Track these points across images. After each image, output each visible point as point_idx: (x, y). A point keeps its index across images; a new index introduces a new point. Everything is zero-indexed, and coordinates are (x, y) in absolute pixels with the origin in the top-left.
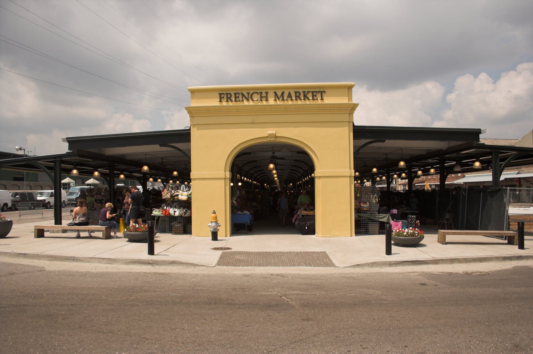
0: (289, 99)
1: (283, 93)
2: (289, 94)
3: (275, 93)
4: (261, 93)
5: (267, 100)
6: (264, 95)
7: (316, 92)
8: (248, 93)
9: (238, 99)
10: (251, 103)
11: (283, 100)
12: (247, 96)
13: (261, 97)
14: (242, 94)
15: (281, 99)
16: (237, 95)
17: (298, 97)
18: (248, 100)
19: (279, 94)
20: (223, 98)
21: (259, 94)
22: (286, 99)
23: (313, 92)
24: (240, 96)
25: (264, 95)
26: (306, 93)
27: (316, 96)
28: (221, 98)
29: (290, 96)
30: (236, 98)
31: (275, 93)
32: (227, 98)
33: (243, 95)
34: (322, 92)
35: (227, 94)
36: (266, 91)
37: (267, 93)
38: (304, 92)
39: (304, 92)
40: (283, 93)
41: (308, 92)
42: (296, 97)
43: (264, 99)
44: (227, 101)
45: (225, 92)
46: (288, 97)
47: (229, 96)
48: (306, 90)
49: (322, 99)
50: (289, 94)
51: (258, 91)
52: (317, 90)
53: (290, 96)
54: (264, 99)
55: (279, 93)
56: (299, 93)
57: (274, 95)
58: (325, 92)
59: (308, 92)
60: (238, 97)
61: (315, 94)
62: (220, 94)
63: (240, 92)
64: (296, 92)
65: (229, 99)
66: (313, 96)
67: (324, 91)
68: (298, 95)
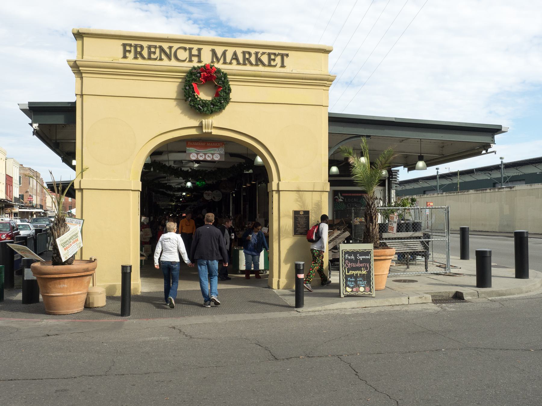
0: (234, 62)
1: (224, 54)
2: (235, 54)
3: (213, 52)
4: (190, 49)
6: (195, 52)
7: (275, 54)
8: (170, 48)
9: (153, 56)
10: (174, 62)
11: (225, 63)
12: (168, 51)
13: (191, 55)
14: (160, 47)
15: (222, 61)
16: (153, 50)
17: (247, 61)
18: (169, 58)
19: (219, 54)
20: (130, 51)
21: (188, 51)
23: (269, 55)
24: (158, 51)
25: (195, 52)
26: (259, 55)
27: (274, 60)
28: (125, 51)
29: (235, 56)
30: (150, 53)
31: (213, 52)
32: (136, 52)
33: (162, 49)
34: (282, 56)
35: (136, 46)
37: (199, 50)
38: (257, 54)
40: (224, 54)
41: (263, 53)
42: (244, 59)
43: (195, 59)
44: (136, 58)
45: (133, 43)
46: (233, 59)
47: (139, 49)
49: (283, 66)
50: (235, 54)
51: (188, 46)
52: (277, 52)
53: (235, 56)
54: (195, 59)
55: (219, 50)
56: (250, 54)
57: (210, 54)
58: (287, 55)
59: (263, 53)
60: (154, 53)
61: (273, 57)
62: (124, 45)
63: (158, 44)
64: (244, 53)
65: (138, 54)
66: (270, 60)
68: (247, 56)
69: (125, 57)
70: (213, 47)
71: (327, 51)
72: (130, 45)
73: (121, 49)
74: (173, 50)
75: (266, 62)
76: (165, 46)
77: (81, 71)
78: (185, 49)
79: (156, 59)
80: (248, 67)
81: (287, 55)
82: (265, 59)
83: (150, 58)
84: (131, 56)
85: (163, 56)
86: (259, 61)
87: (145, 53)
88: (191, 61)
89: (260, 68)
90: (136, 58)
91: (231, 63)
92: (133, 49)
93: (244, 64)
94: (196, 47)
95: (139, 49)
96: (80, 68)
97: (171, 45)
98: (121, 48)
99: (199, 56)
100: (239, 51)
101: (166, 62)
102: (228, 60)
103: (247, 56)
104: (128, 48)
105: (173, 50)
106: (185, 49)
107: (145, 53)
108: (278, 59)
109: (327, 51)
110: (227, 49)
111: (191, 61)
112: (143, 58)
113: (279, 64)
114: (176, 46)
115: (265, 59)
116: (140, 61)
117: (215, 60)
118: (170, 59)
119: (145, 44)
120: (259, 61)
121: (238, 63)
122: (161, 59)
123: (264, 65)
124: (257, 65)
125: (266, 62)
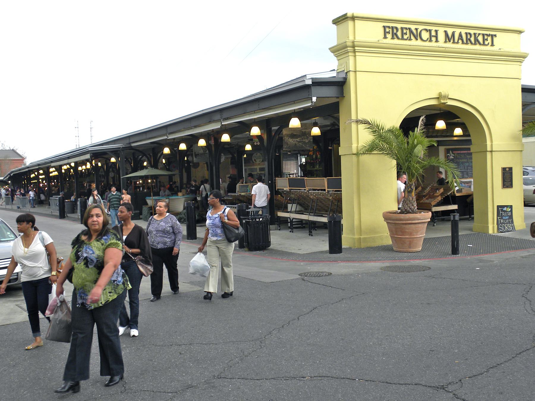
0: (460, 41)
2: (460, 35)
3: (446, 32)
5: (437, 41)
6: (433, 33)
7: (487, 35)
8: (416, 29)
9: (405, 37)
10: (419, 42)
11: (454, 42)
12: (415, 32)
14: (410, 29)
15: (452, 41)
17: (468, 41)
19: (450, 35)
20: (389, 33)
21: (429, 32)
22: (456, 41)
23: (483, 35)
25: (433, 33)
27: (487, 40)
28: (385, 33)
30: (403, 34)
31: (446, 32)
34: (492, 36)
35: (392, 28)
36: (437, 28)
37: (436, 31)
39: (475, 34)
41: (479, 34)
43: (434, 39)
44: (393, 38)
47: (395, 31)
48: (478, 32)
49: (492, 45)
50: (460, 35)
52: (488, 33)
54: (434, 39)
55: (450, 31)
58: (495, 36)
62: (384, 27)
63: (408, 26)
64: (466, 33)
65: (394, 36)
66: (484, 40)
67: (495, 34)
69: (385, 37)
70: (446, 29)
71: (520, 32)
72: (389, 27)
73: (382, 31)
74: (419, 31)
75: (481, 41)
76: (413, 27)
77: (356, 50)
78: (426, 30)
79: (406, 39)
80: (469, 47)
81: (495, 36)
82: (480, 38)
83: (403, 39)
84: (389, 36)
85: (412, 37)
86: (477, 41)
87: (399, 34)
88: (431, 41)
89: (477, 47)
90: (393, 38)
91: (458, 43)
92: (391, 30)
93: (467, 43)
94: (434, 28)
95: (395, 31)
96: (356, 48)
97: (417, 27)
98: (382, 29)
99: (436, 37)
100: (463, 31)
101: (413, 42)
102: (456, 41)
103: (469, 37)
104: (387, 30)
105: (419, 31)
106: (426, 30)
107: (399, 34)
108: (489, 39)
109: (520, 32)
110: (454, 31)
111: (431, 41)
112: (398, 38)
113: (490, 44)
114: (420, 28)
115: (480, 38)
116: (396, 41)
117: (447, 40)
118: (417, 39)
119: (399, 26)
120: (477, 41)
121: (463, 43)
122: (410, 39)
123: (480, 44)
124: (475, 44)
125: (481, 41)
